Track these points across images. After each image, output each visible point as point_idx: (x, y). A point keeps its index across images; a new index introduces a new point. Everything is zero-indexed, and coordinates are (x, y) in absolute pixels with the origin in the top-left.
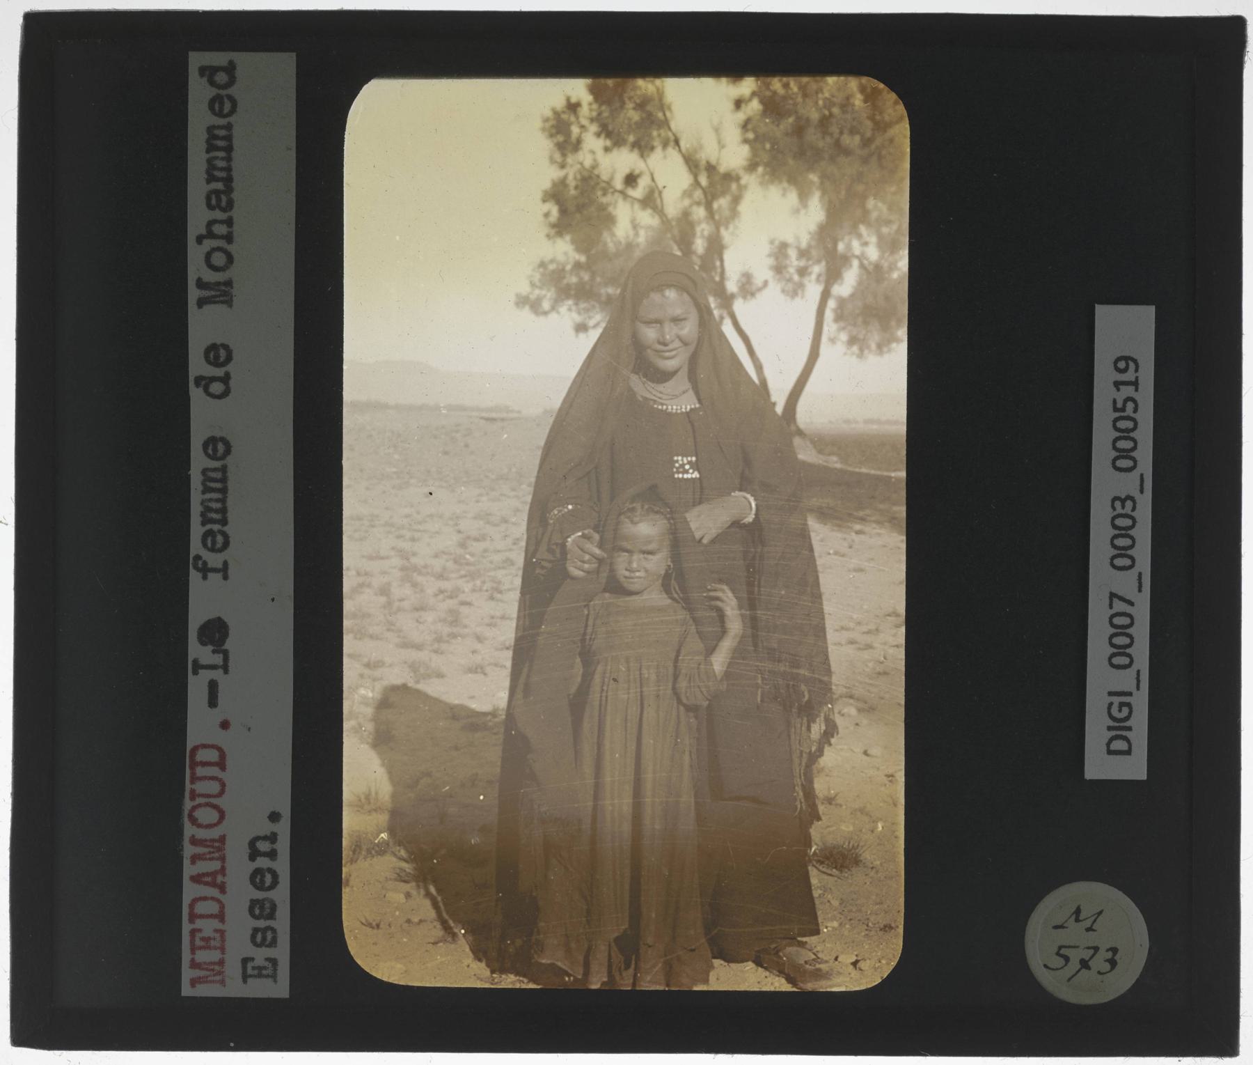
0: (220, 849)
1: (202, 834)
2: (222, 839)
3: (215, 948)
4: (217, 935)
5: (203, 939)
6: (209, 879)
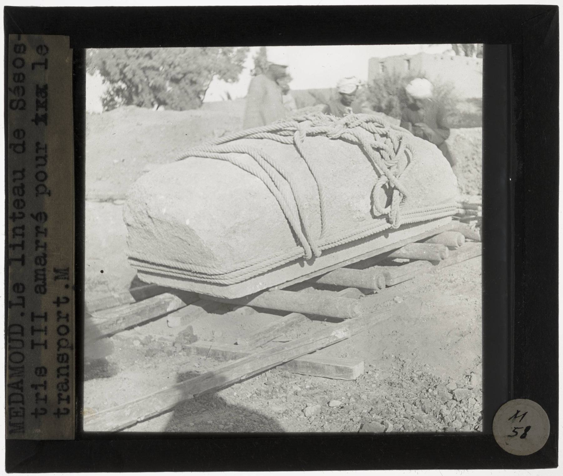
2: (23, 367)
3: (21, 416)
4: (21, 410)
5: (14, 412)
6: (15, 386)
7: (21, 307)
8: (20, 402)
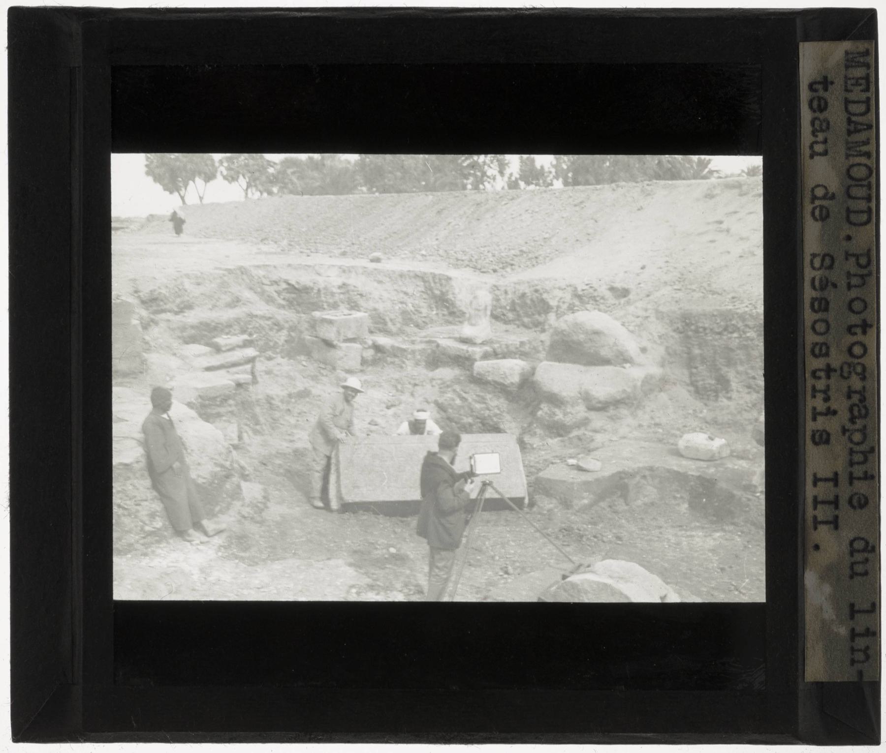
0: (849, 149)
1: (863, 160)
4: (849, 87)
5: (860, 85)
7: (852, 208)
8: (854, 102)
